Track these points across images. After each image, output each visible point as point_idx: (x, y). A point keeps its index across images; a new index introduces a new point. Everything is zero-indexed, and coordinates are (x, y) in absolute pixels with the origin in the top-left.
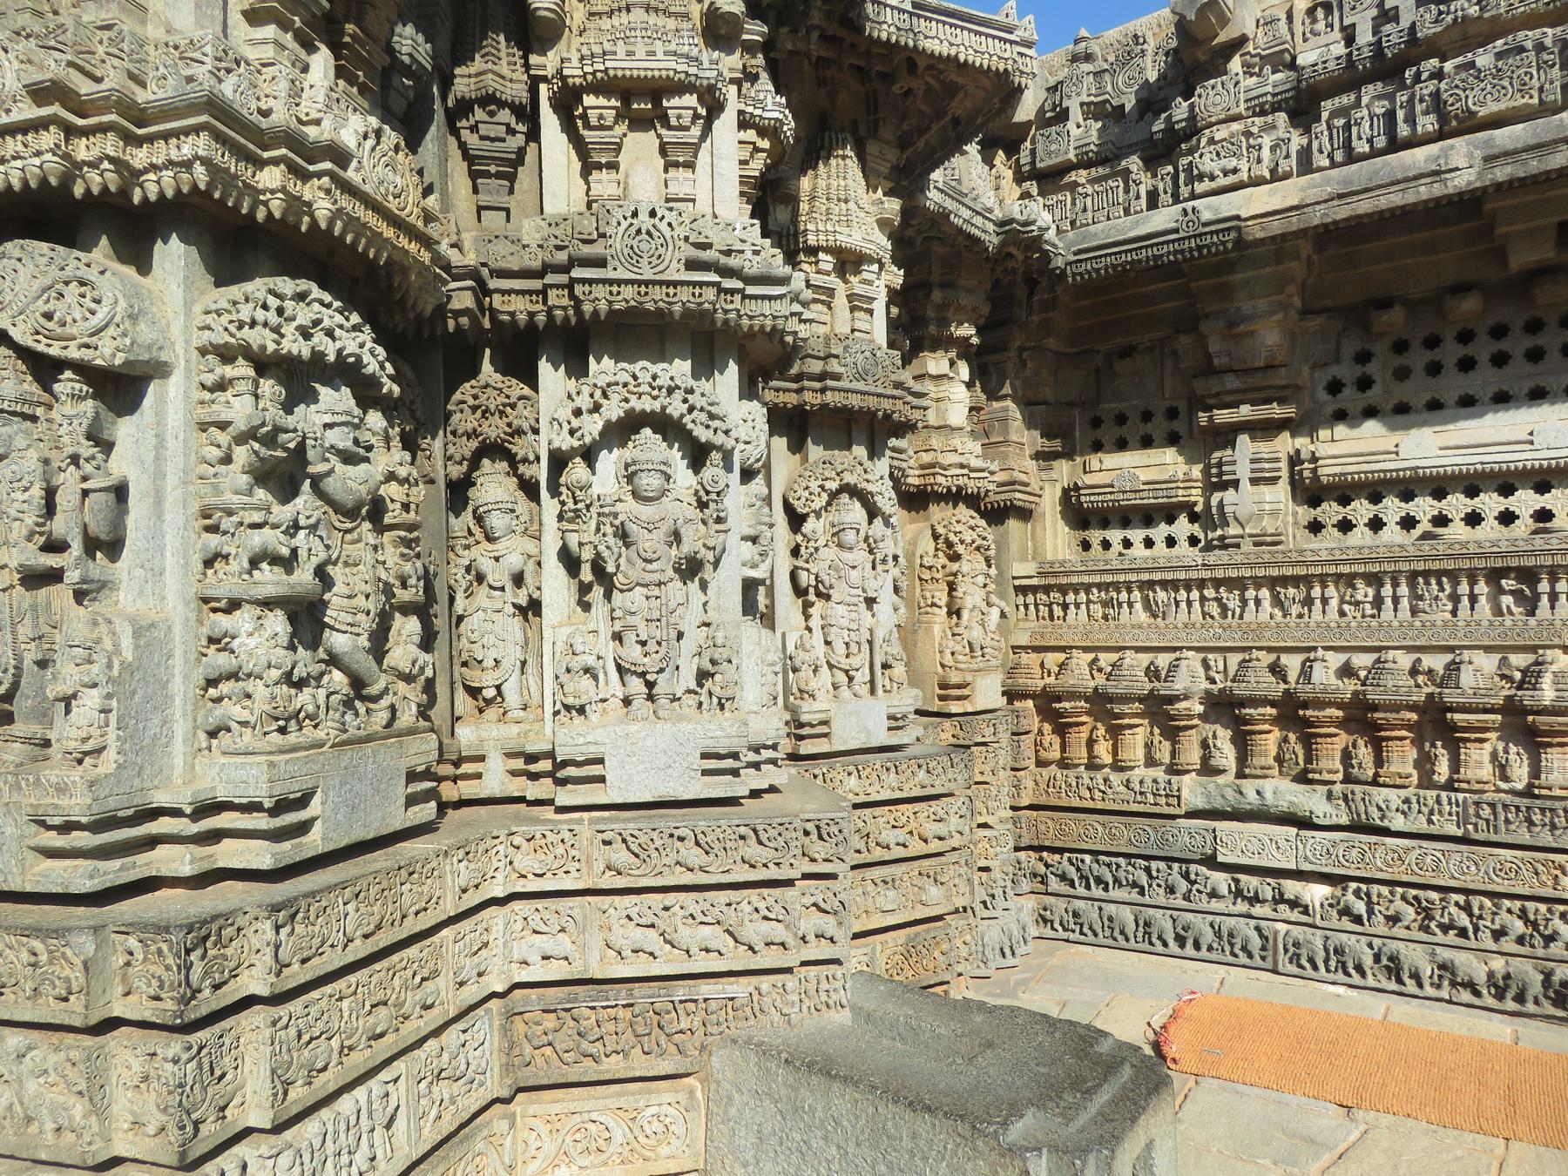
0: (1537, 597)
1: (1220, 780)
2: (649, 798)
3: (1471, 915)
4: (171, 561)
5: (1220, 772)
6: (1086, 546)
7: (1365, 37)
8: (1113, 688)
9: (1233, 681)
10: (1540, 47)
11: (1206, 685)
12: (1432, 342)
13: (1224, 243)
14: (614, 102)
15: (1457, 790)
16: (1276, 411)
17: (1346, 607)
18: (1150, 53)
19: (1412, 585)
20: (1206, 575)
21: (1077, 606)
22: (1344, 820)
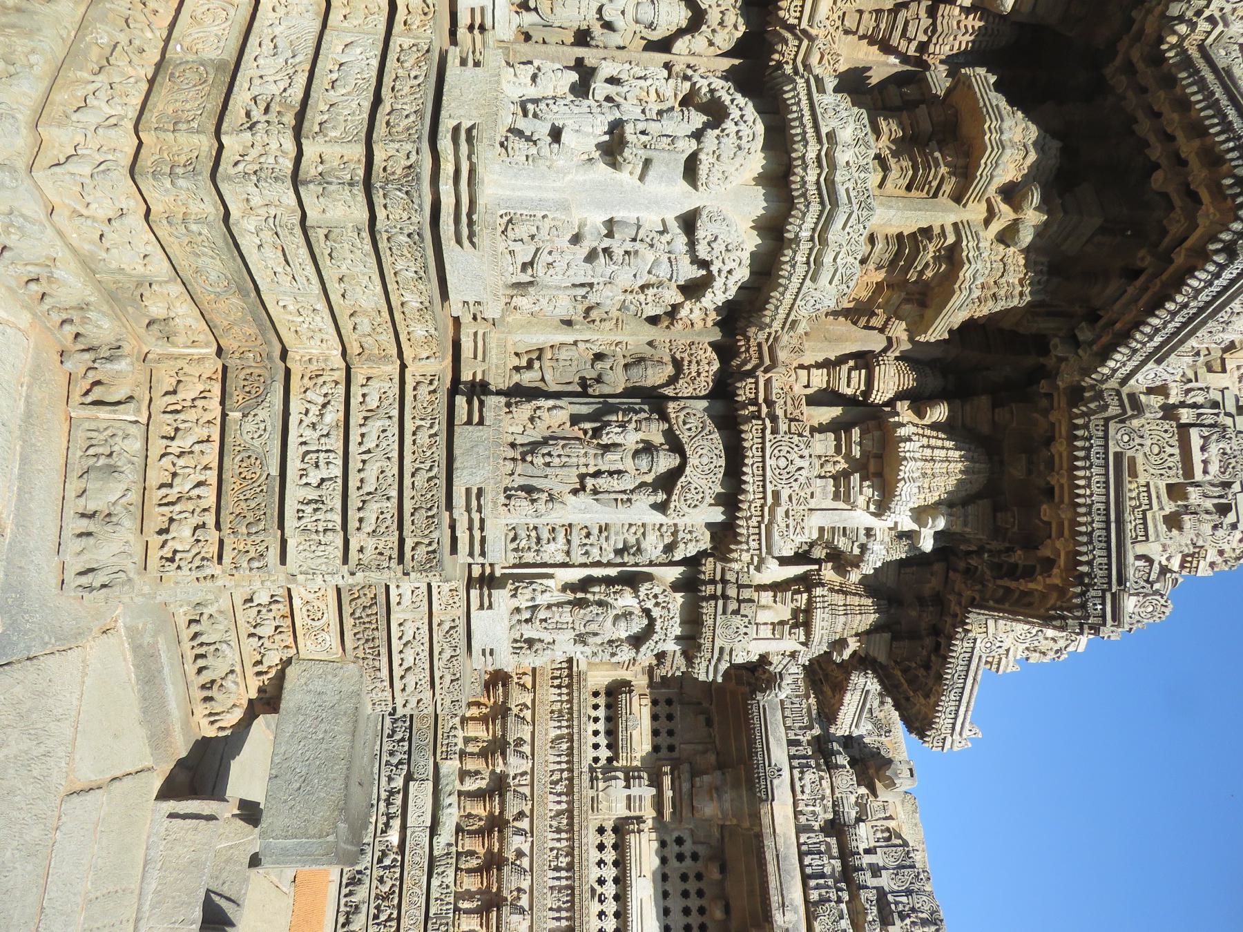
1: (457, 782)
2: (473, 627)
3: (386, 921)
4: (588, 516)
5: (462, 782)
6: (596, 694)
7: (867, 860)
11: (512, 774)
12: (700, 893)
13: (760, 791)
14: (803, 607)
15: (454, 913)
16: (668, 811)
17: (555, 852)
18: (880, 739)
19: (567, 887)
20: (576, 774)
21: (560, 695)
22: (436, 853)
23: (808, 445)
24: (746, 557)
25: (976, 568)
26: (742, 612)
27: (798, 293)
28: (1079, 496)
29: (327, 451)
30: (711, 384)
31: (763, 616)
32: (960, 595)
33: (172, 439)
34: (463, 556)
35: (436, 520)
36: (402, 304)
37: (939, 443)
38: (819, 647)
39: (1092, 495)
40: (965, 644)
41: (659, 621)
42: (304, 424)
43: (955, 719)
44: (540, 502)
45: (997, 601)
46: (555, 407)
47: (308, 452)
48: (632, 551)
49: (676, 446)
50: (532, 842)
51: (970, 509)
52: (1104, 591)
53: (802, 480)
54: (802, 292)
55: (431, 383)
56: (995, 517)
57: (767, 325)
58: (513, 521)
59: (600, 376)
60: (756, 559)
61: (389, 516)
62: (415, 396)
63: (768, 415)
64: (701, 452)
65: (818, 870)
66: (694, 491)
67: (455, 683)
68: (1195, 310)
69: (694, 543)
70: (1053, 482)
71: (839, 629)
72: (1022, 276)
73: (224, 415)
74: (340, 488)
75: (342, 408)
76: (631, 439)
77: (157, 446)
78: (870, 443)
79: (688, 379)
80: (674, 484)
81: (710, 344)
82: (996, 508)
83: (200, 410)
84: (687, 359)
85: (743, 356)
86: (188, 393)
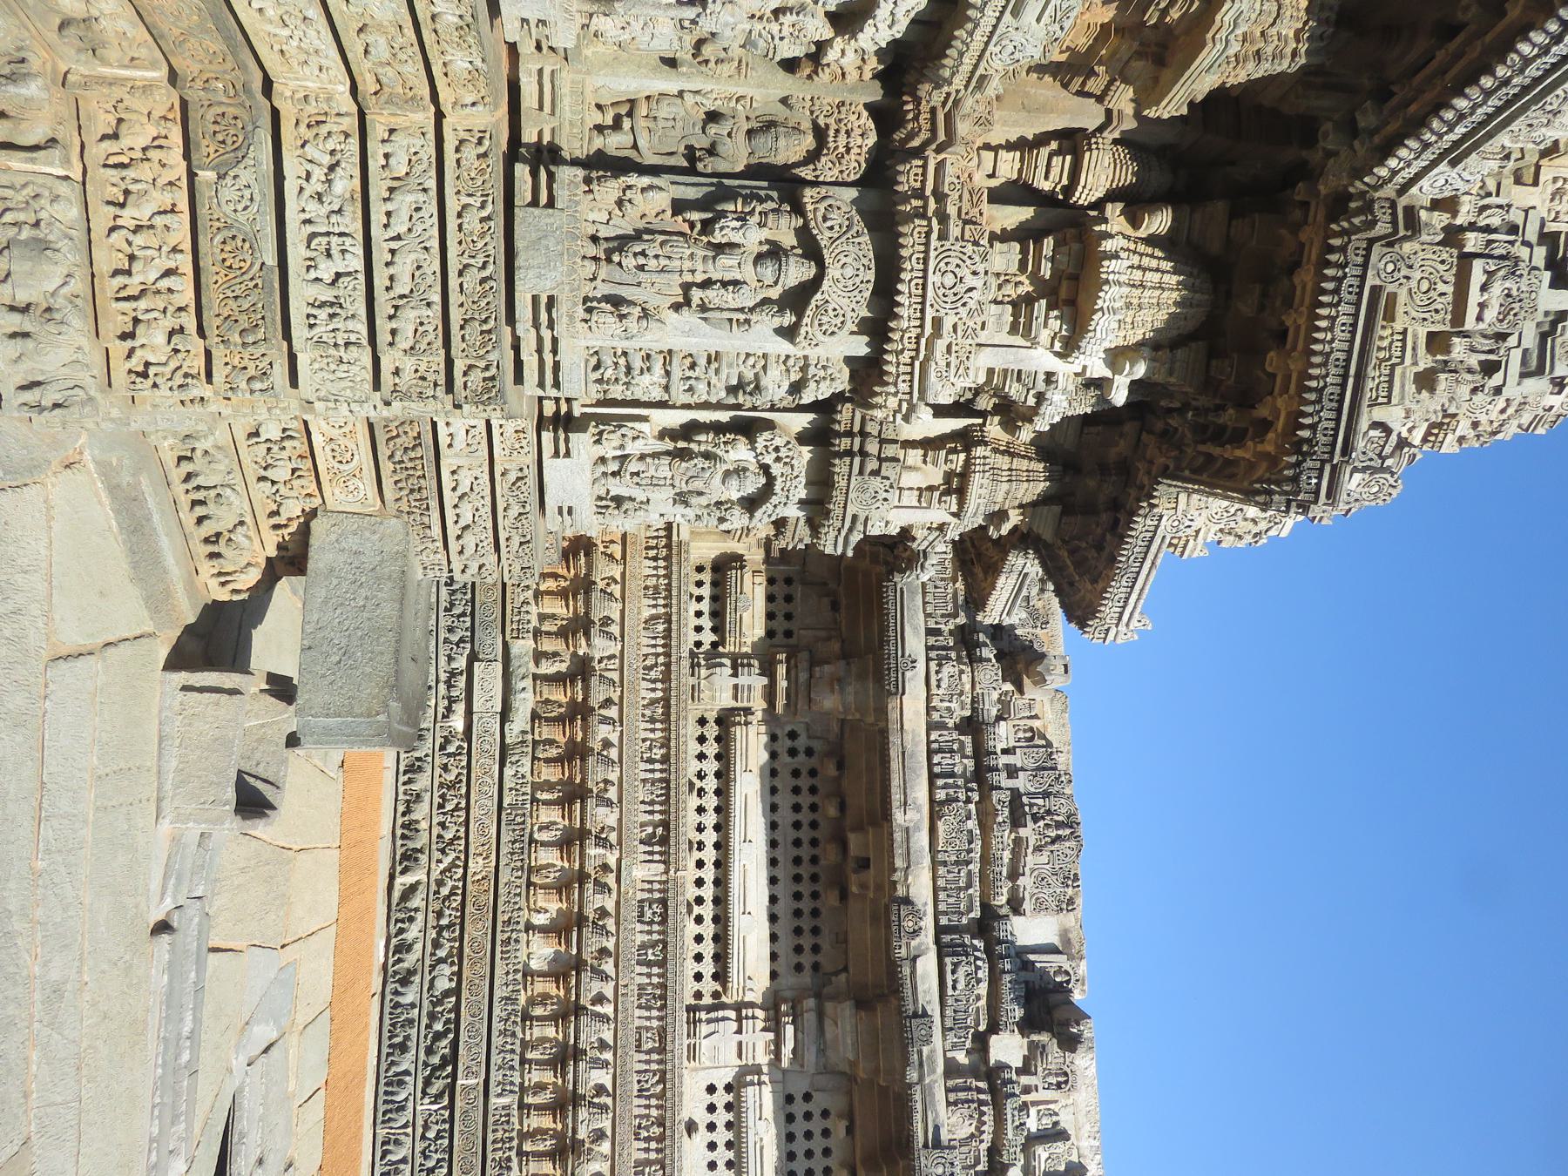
0: (652, 845)
1: (532, 665)
3: (453, 810)
4: (694, 340)
5: (537, 664)
6: (700, 569)
7: (1004, 760)
8: (595, 596)
9: (600, 676)
10: (970, 851)
11: (597, 657)
14: (959, 470)
16: (781, 702)
19: (661, 780)
20: (673, 659)
21: (656, 568)
22: (508, 741)
23: (984, 259)
24: (892, 402)
25: (1176, 429)
26: (883, 473)
27: (992, 33)
28: (1317, 341)
29: (341, 234)
30: (864, 165)
31: (909, 479)
32: (1151, 462)
33: (122, 206)
34: (530, 387)
35: (494, 337)
36: (433, 17)
37: (1154, 263)
38: (973, 519)
39: (1332, 341)
40: (1149, 522)
41: (779, 480)
42: (307, 193)
43: (1124, 607)
44: (630, 318)
45: (1194, 471)
46: (651, 187)
47: (313, 236)
48: (749, 389)
49: (811, 250)
50: (622, 732)
51: (1179, 353)
52: (1323, 462)
53: (972, 304)
54: (998, 32)
55: (480, 142)
56: (1208, 365)
57: (945, 80)
58: (596, 344)
59: (713, 144)
60: (905, 405)
61: (431, 328)
62: (458, 161)
63: (936, 212)
64: (844, 260)
65: (947, 769)
66: (831, 313)
67: (525, 546)
68: (1516, 90)
69: (828, 382)
70: (1289, 323)
71: (1000, 499)
72: (1300, 25)
73: (191, 175)
74: (362, 288)
75: (357, 172)
76: (753, 238)
77: (102, 217)
78: (1065, 259)
79: (833, 157)
80: (807, 303)
81: (866, 106)
82: (1213, 353)
83: (156, 165)
84: (833, 127)
85: (910, 126)
86: (136, 137)
